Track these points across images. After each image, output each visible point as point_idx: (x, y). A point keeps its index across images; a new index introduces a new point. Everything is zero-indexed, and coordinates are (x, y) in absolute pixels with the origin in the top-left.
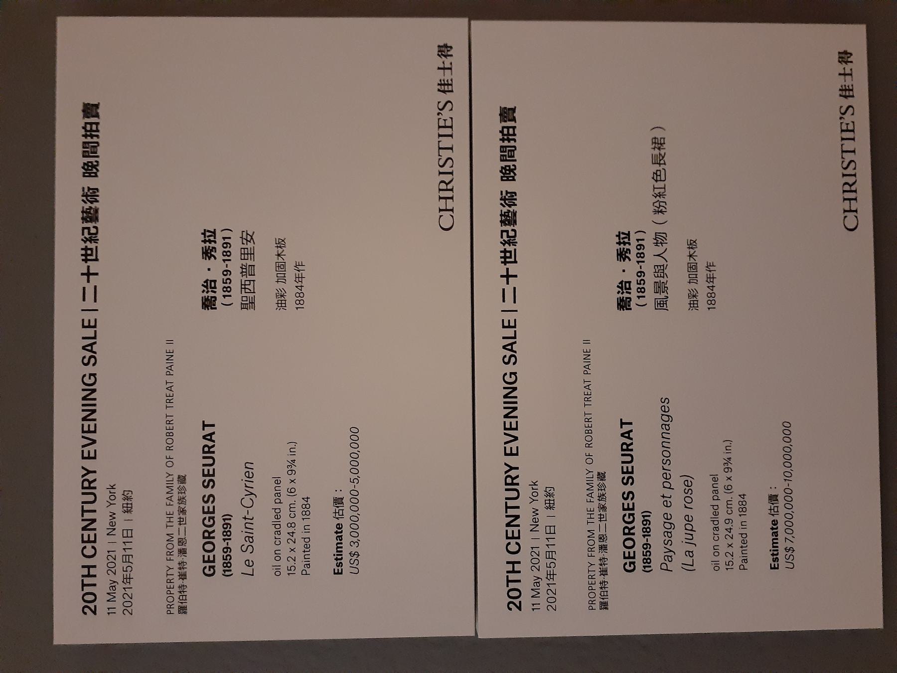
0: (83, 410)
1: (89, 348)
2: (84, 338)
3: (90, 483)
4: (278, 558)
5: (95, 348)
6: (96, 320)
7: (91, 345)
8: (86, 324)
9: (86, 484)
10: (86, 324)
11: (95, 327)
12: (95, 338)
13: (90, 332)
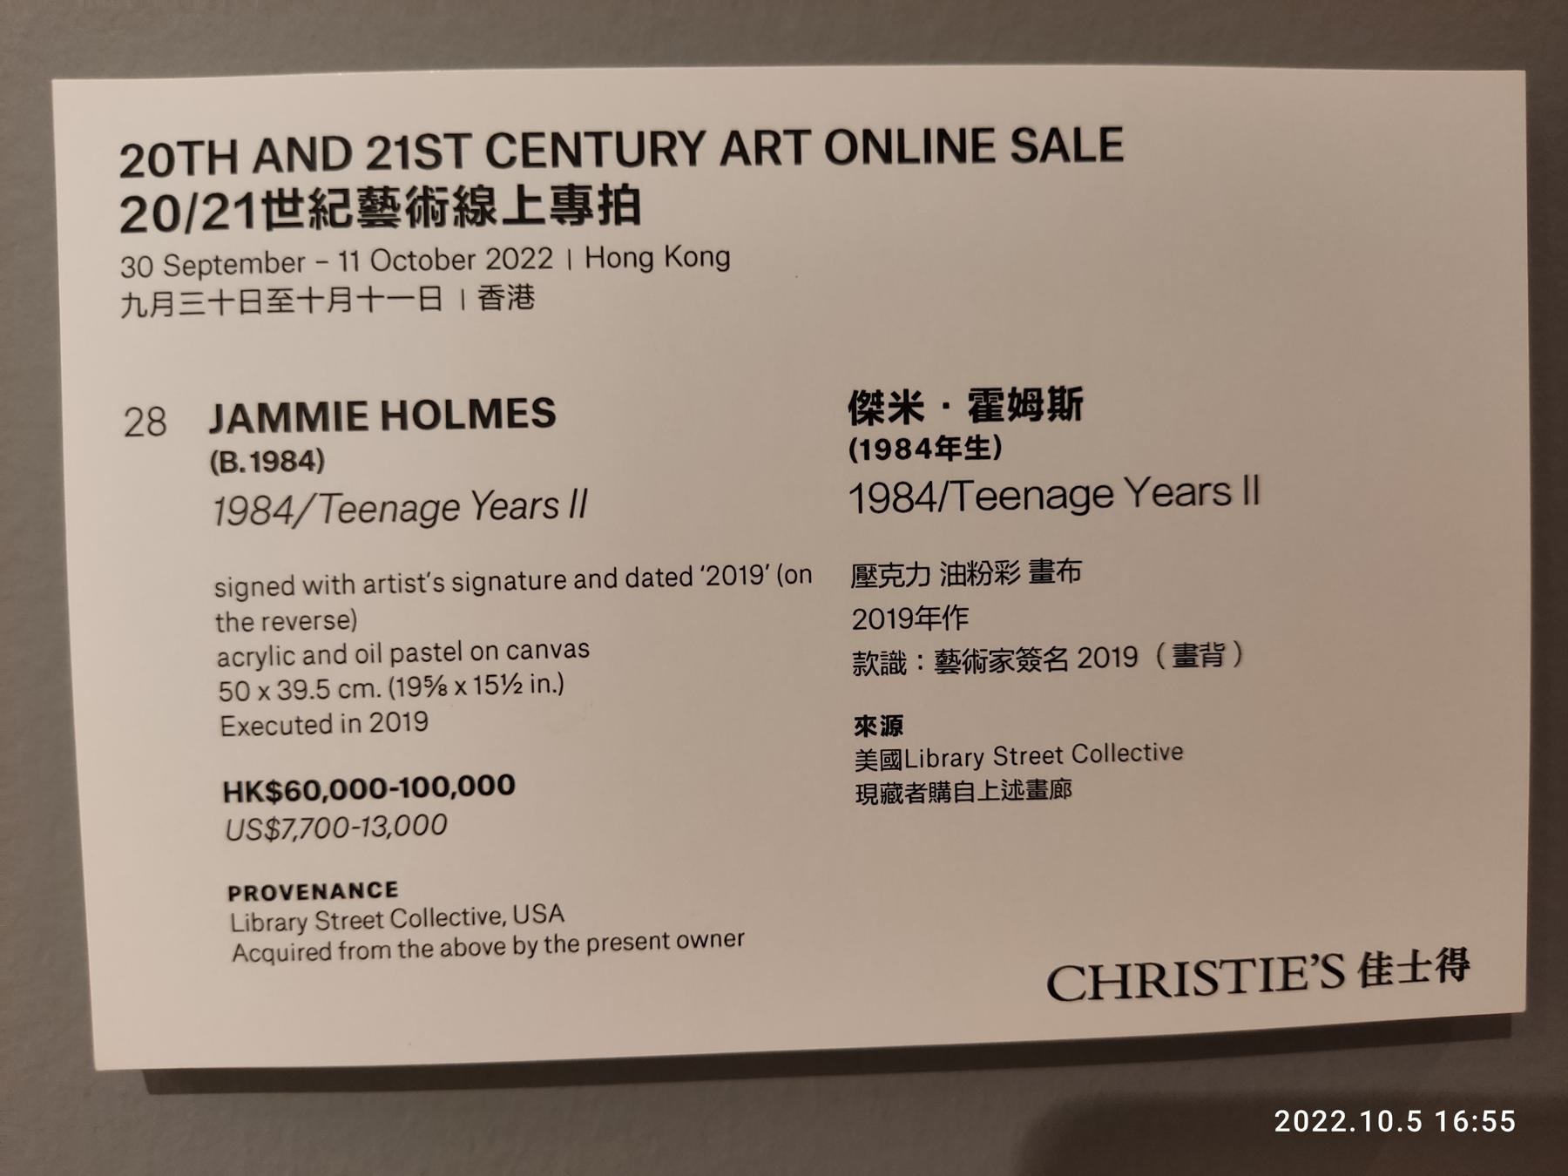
0: (888, 132)
1: (1055, 144)
2: (1077, 131)
3: (667, 151)
4: (477, 653)
5: (1055, 158)
6: (1120, 159)
7: (1062, 149)
8: (1111, 137)
9: (663, 142)
10: (1111, 137)
11: (1105, 157)
12: (1079, 158)
13: (1091, 146)
